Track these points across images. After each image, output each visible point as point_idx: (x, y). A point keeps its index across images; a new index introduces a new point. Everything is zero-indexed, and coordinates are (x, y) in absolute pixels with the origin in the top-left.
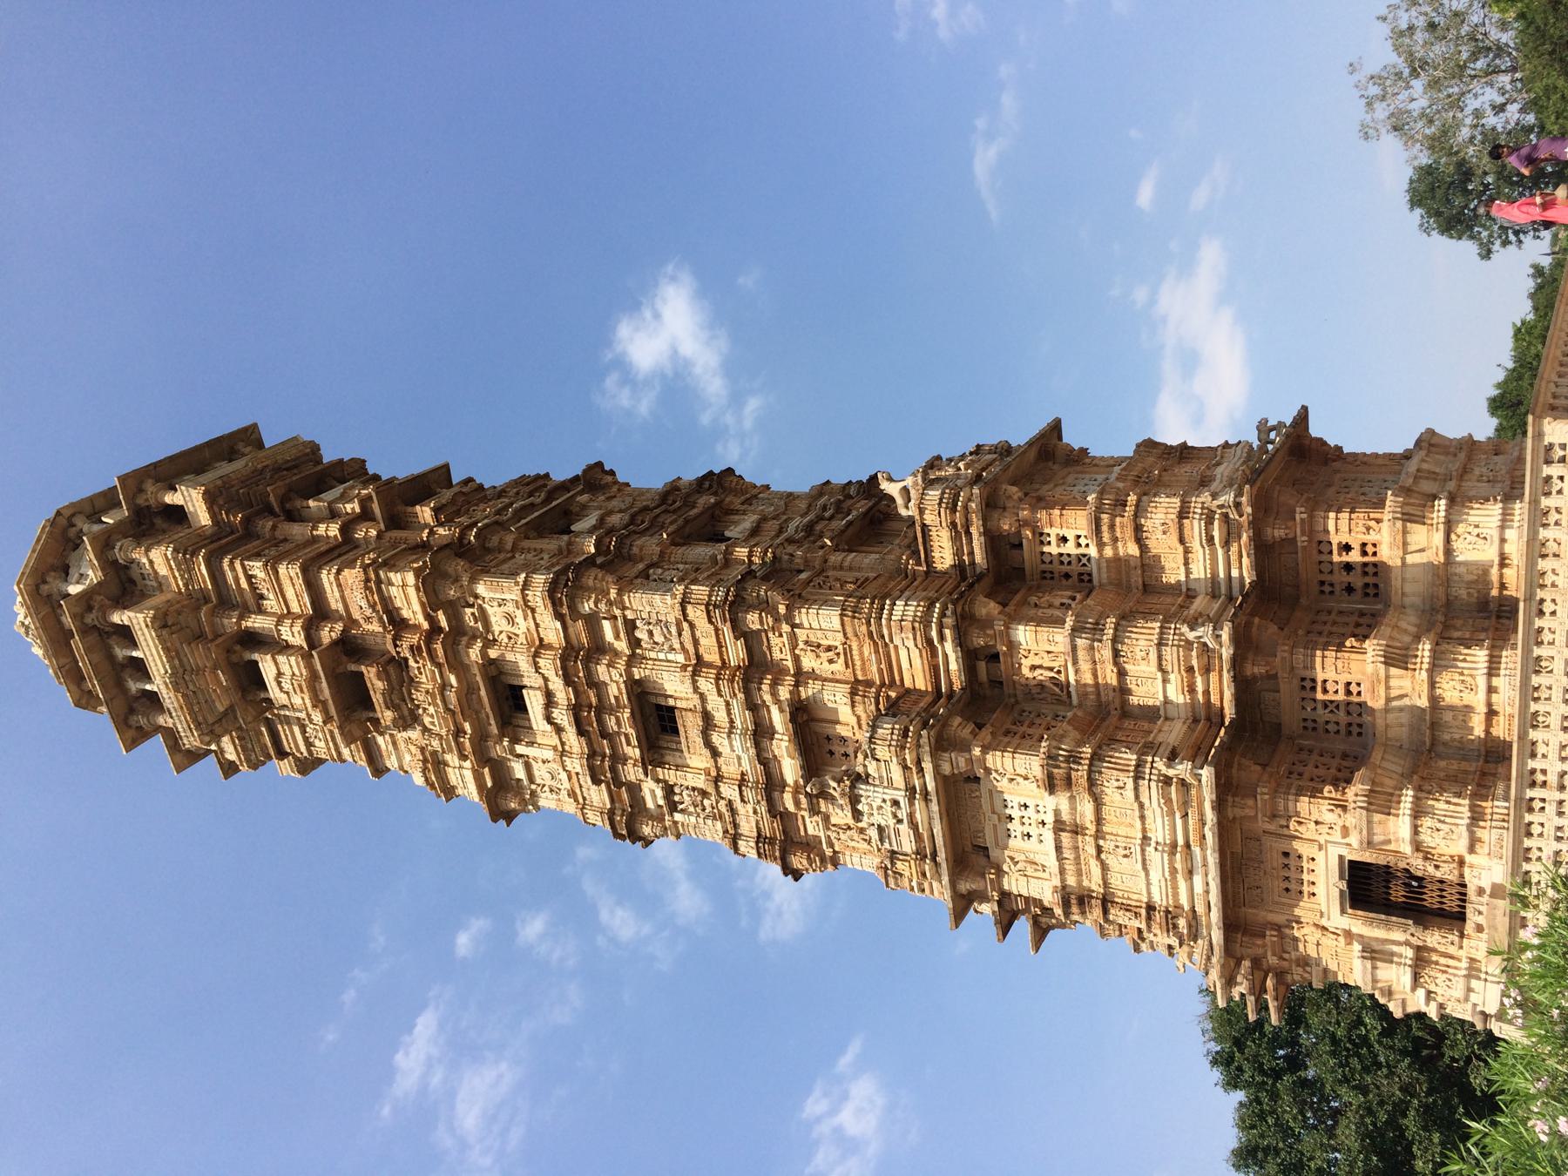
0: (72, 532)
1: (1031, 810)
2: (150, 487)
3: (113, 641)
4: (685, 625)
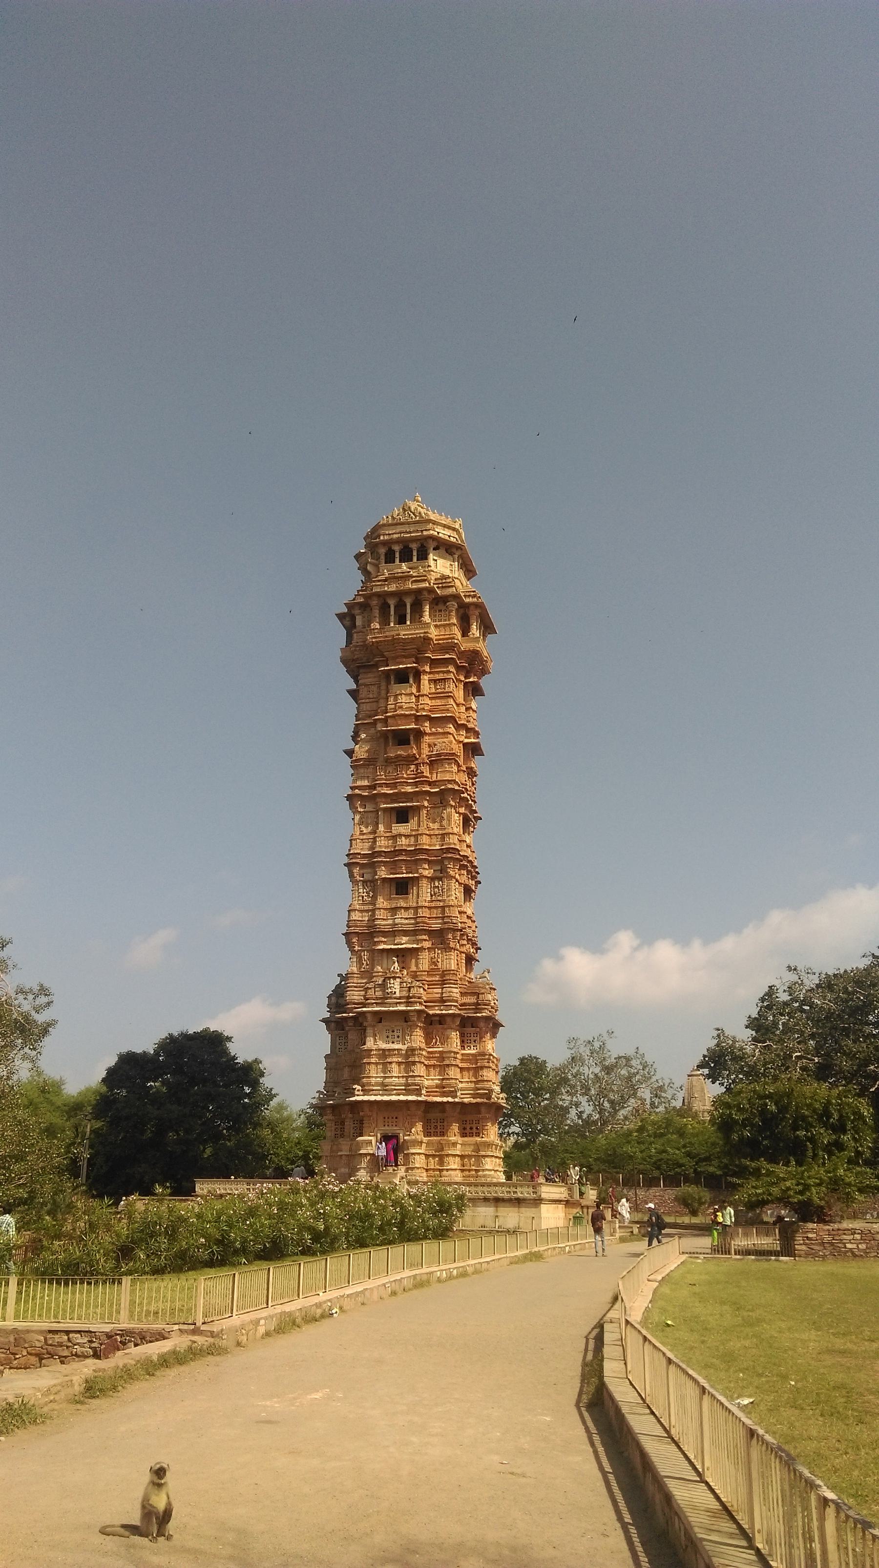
0: (454, 550)
1: (396, 1039)
2: (477, 612)
3: (413, 597)
4: (442, 904)
